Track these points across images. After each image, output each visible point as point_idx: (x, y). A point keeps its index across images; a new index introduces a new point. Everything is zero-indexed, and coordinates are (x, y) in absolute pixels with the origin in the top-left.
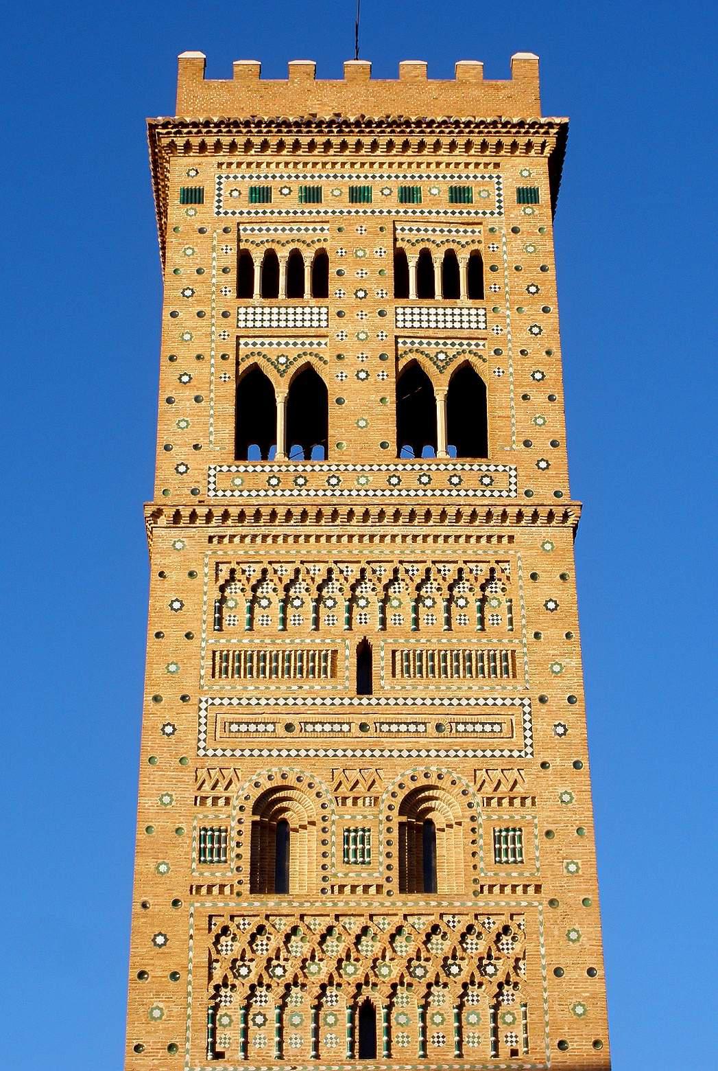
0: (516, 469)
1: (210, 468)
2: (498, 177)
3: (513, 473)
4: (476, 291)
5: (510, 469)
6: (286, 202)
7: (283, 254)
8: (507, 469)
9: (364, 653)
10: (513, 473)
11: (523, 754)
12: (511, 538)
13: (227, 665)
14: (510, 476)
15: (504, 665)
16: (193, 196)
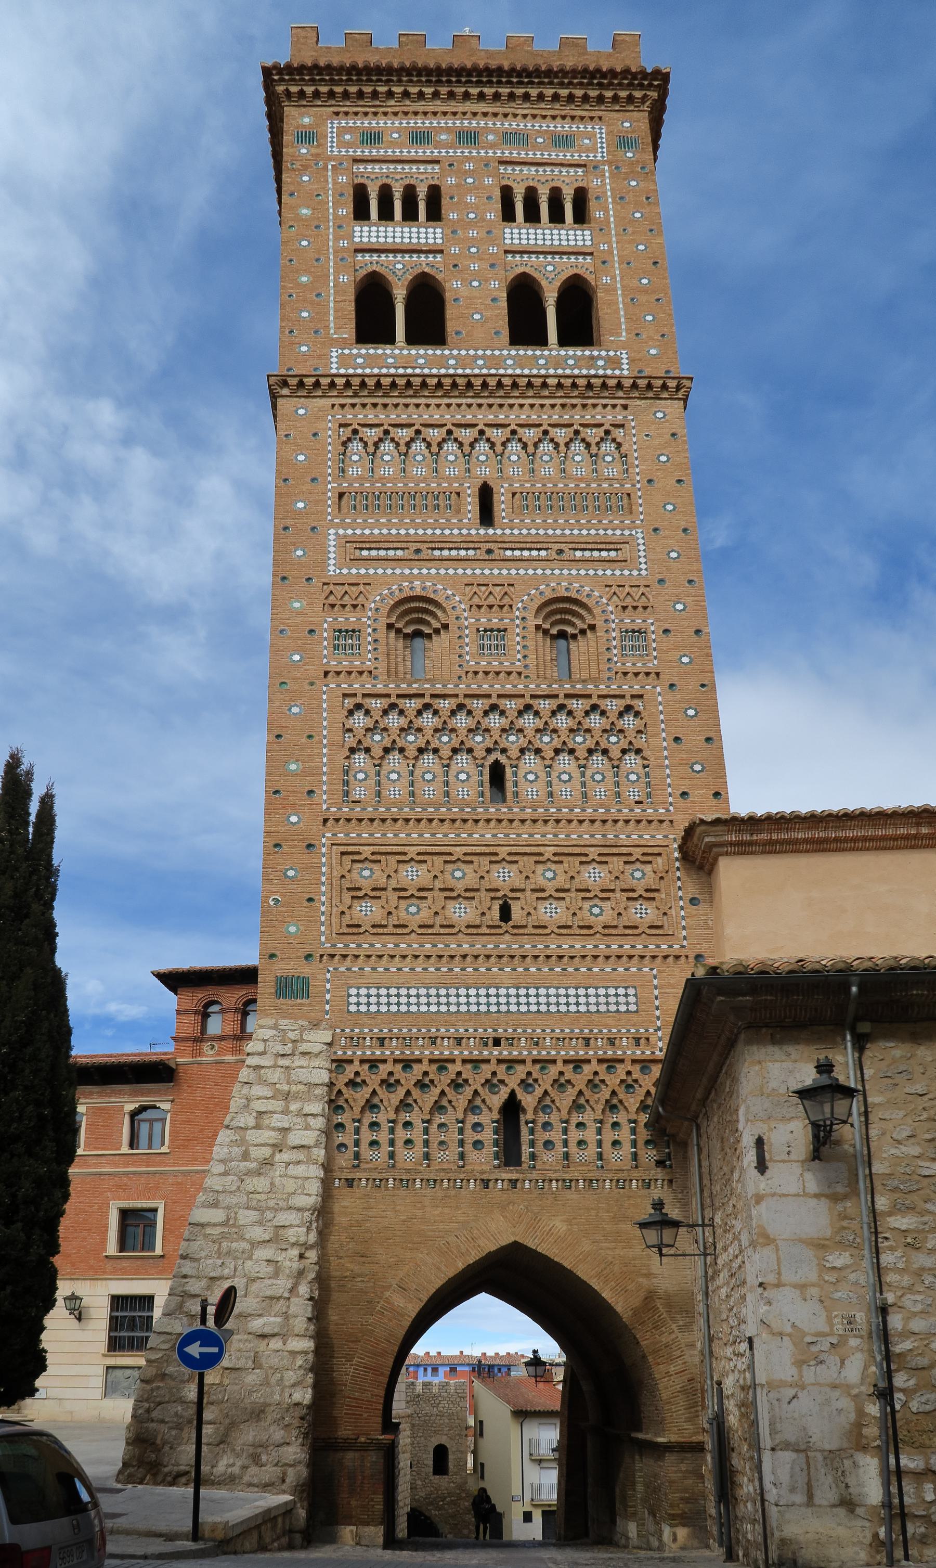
16: (306, 137)
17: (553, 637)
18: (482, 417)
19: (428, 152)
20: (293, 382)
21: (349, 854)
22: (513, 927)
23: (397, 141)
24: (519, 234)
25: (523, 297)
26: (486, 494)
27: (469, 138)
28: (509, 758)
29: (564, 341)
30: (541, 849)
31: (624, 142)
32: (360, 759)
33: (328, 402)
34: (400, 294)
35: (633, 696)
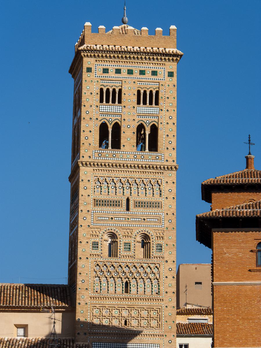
0: (163, 154)
1: (93, 151)
2: (164, 68)
3: (163, 156)
4: (157, 103)
5: (162, 154)
6: (112, 73)
7: (111, 90)
8: (161, 154)
9: (128, 200)
10: (163, 156)
11: (162, 226)
12: (163, 173)
13: (97, 203)
14: (162, 156)
15: (158, 205)
16: (89, 70)
28: (129, 280)
31: (171, 74)
34: (110, 130)
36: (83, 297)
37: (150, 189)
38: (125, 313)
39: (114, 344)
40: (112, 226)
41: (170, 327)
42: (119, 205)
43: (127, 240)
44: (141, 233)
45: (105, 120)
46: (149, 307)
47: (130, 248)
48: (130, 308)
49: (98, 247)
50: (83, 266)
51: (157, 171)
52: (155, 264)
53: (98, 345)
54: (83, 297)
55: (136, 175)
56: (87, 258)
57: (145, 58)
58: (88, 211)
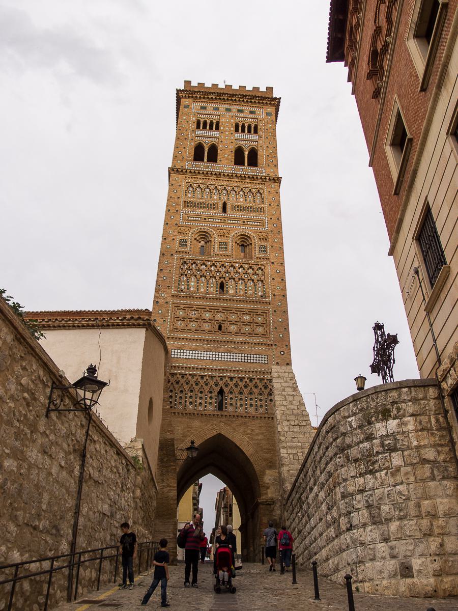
7: (208, 121)
15: (261, 210)
16: (187, 106)
17: (240, 245)
18: (225, 183)
19: (218, 113)
20: (175, 170)
21: (177, 306)
22: (223, 332)
23: (210, 111)
24: (239, 135)
25: (239, 152)
26: (225, 205)
27: (228, 110)
29: (249, 165)
30: (231, 309)
32: (184, 278)
33: (184, 176)
34: (206, 149)
35: (261, 265)
36: (163, 295)
37: (250, 197)
38: (220, 317)
39: (202, 353)
40: (204, 226)
41: (281, 336)
42: (214, 208)
43: (223, 240)
44: (240, 234)
45: (201, 142)
46: (252, 311)
47: (226, 248)
48: (226, 310)
49: (186, 245)
50: (166, 262)
51: (258, 182)
52: (258, 265)
53: (180, 352)
54: (163, 295)
55: (234, 184)
56: (172, 255)
57: (243, 101)
58: (177, 211)
